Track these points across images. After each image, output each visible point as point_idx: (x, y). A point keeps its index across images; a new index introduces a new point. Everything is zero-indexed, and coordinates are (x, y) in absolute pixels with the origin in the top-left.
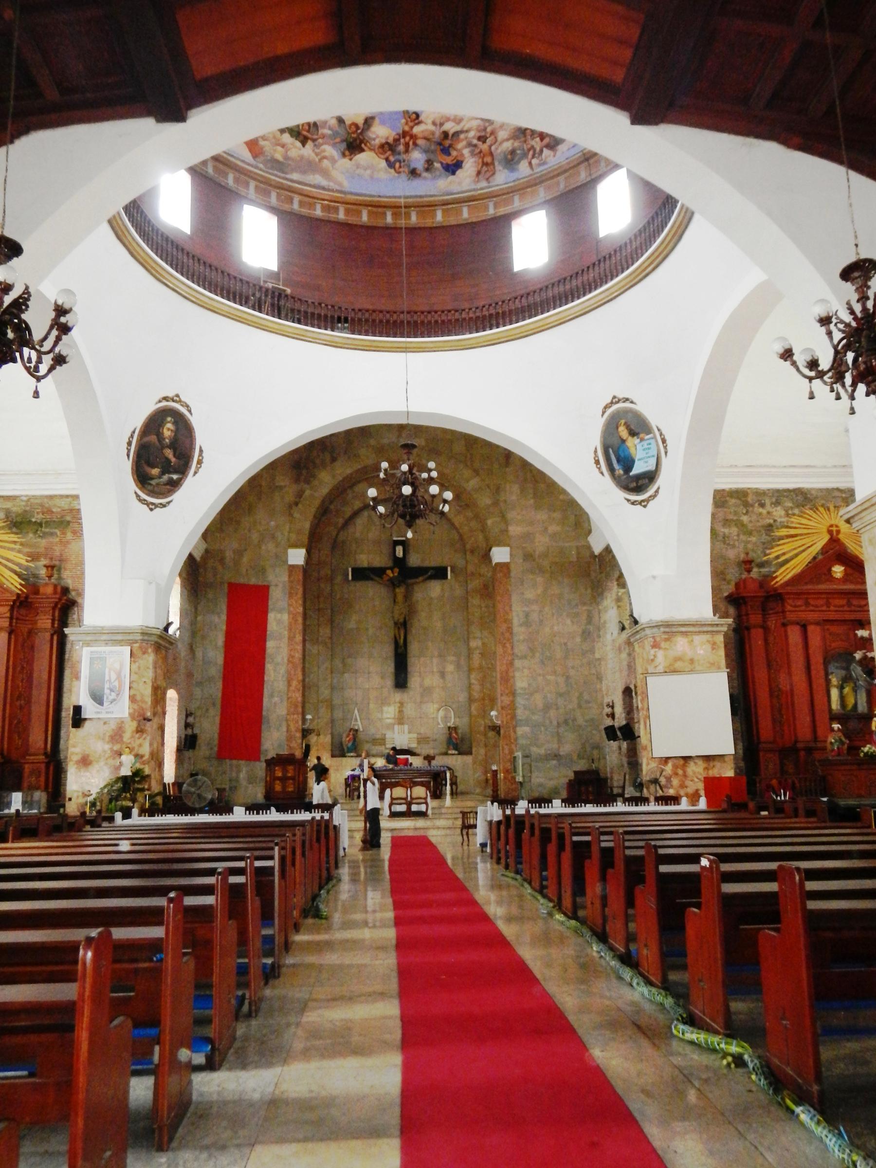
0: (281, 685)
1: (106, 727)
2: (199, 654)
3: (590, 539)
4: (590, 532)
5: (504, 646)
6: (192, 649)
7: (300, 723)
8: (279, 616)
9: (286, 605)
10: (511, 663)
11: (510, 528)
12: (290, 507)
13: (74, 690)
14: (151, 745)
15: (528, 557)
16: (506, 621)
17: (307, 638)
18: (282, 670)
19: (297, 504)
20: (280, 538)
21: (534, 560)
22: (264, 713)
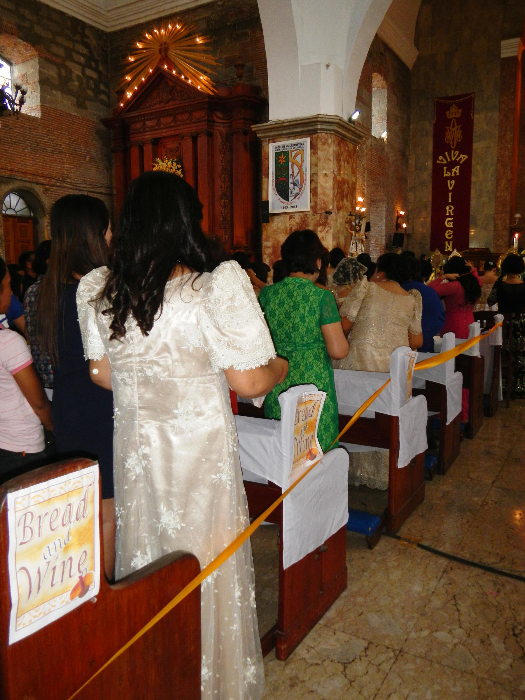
0: (490, 186)
1: (292, 222)
2: (412, 161)
6: (404, 156)
7: (508, 221)
13: (264, 186)
14: (334, 238)
18: (492, 170)
22: (471, 213)
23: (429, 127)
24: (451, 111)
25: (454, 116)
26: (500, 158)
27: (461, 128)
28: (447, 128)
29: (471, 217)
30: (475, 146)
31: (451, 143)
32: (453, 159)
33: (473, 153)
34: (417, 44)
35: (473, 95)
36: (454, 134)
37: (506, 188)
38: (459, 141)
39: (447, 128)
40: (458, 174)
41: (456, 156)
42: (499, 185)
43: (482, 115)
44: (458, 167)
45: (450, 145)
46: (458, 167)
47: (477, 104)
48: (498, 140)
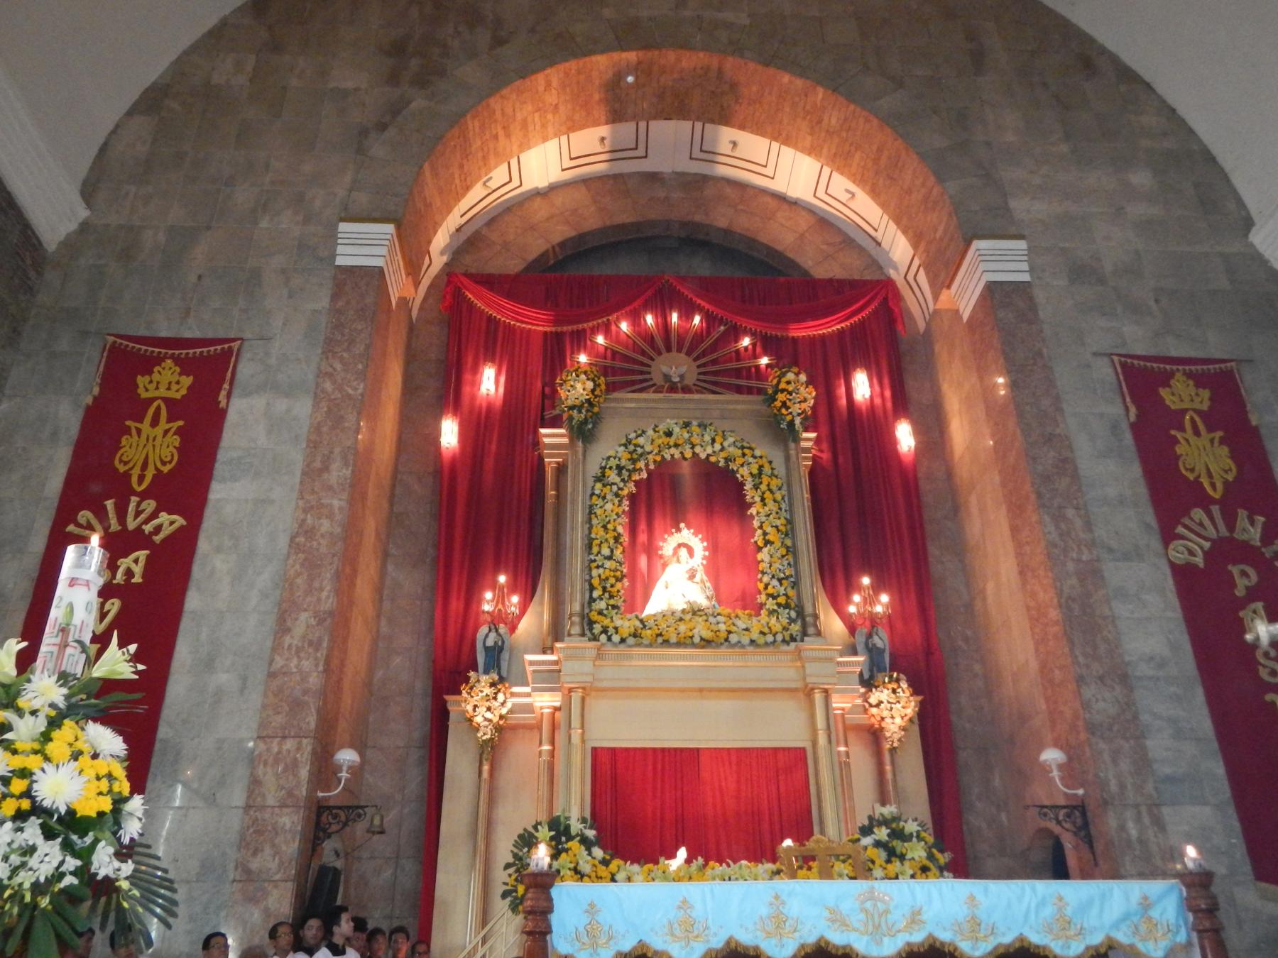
3: (1258, 238)
4: (1248, 223)
5: (1059, 518)
7: (304, 773)
8: (281, 405)
9: (311, 377)
10: (1091, 574)
11: (1013, 204)
12: (364, 132)
15: (1081, 273)
16: (1049, 439)
17: (393, 551)
18: (265, 577)
19: (382, 127)
20: (318, 203)
21: (1102, 281)
23: (68, 417)
24: (156, 377)
25: (162, 392)
26: (301, 539)
27: (179, 432)
28: (128, 423)
29: (158, 746)
30: (217, 492)
31: (135, 474)
32: (132, 524)
33: (209, 513)
34: (88, 192)
35: (235, 345)
36: (150, 447)
37: (311, 643)
38: (166, 469)
39: (128, 423)
40: (137, 579)
41: (143, 516)
42: (289, 630)
43: (259, 402)
44: (142, 554)
45: (130, 476)
46: (142, 554)
47: (246, 369)
48: (301, 483)
